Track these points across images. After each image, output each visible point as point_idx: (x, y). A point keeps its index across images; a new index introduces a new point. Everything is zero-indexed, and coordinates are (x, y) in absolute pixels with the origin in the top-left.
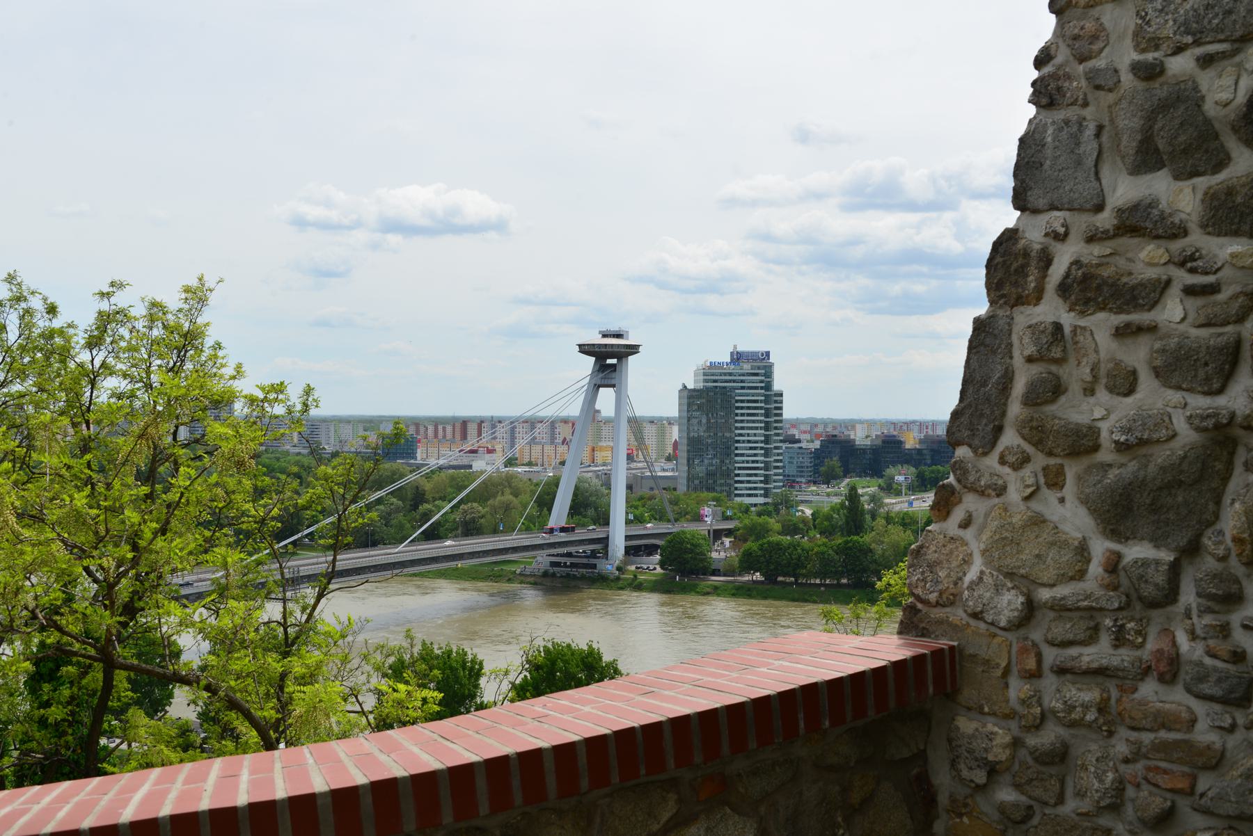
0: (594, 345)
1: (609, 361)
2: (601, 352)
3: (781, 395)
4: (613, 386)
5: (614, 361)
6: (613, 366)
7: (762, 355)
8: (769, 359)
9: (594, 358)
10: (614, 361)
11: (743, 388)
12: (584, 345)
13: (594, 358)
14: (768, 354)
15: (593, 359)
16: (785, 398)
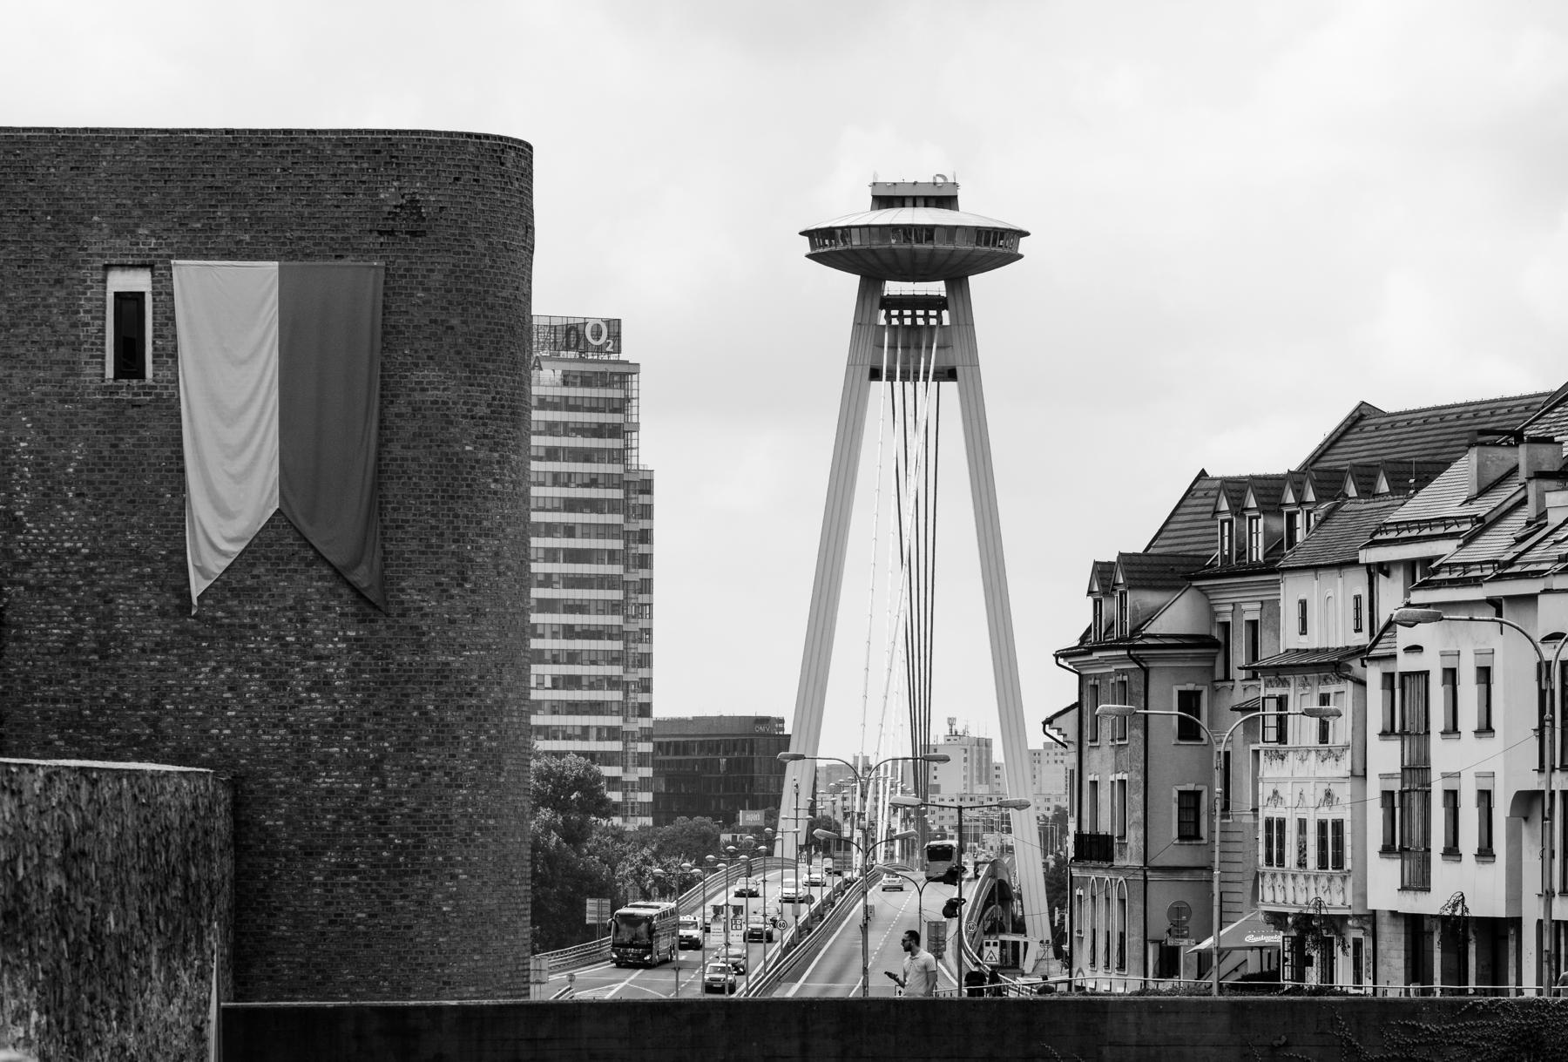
0: (846, 231)
1: (893, 288)
2: (932, 253)
3: (646, 487)
4: (951, 375)
5: (937, 288)
6: (937, 303)
7: (598, 335)
8: (619, 352)
9: (859, 277)
10: (937, 288)
12: (829, 233)
13: (856, 279)
14: (614, 329)
15: (852, 281)
16: (662, 500)
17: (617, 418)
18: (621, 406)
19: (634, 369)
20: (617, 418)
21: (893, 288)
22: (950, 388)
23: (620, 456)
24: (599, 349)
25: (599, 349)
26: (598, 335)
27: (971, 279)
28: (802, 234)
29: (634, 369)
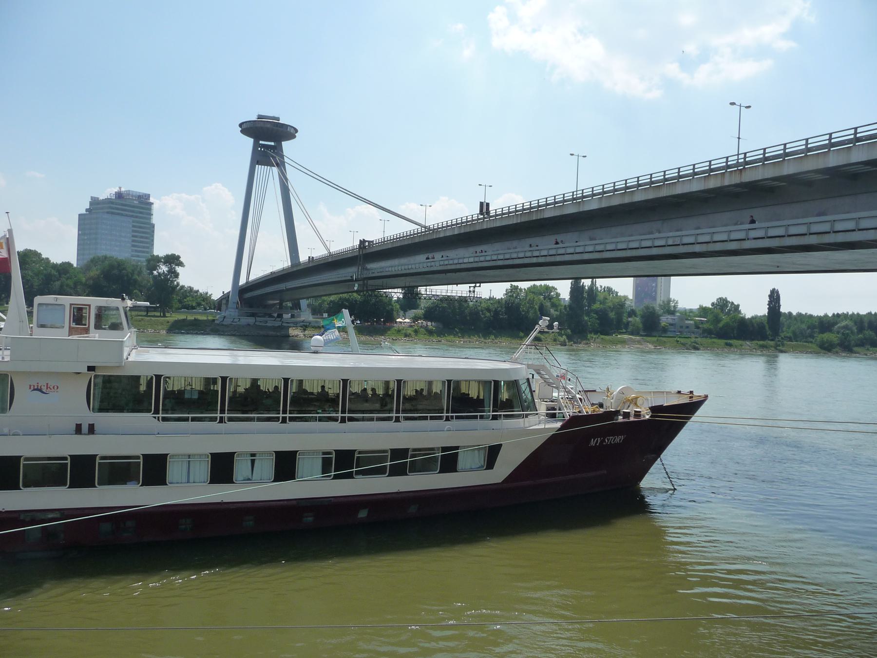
5: (272, 144)
7: (145, 196)
8: (149, 200)
10: (272, 144)
11: (136, 217)
14: (148, 196)
17: (148, 211)
18: (150, 209)
19: (153, 204)
20: (148, 211)
21: (261, 142)
22: (275, 170)
23: (150, 219)
24: (146, 199)
25: (146, 199)
26: (145, 196)
27: (282, 142)
28: (241, 125)
29: (153, 204)
